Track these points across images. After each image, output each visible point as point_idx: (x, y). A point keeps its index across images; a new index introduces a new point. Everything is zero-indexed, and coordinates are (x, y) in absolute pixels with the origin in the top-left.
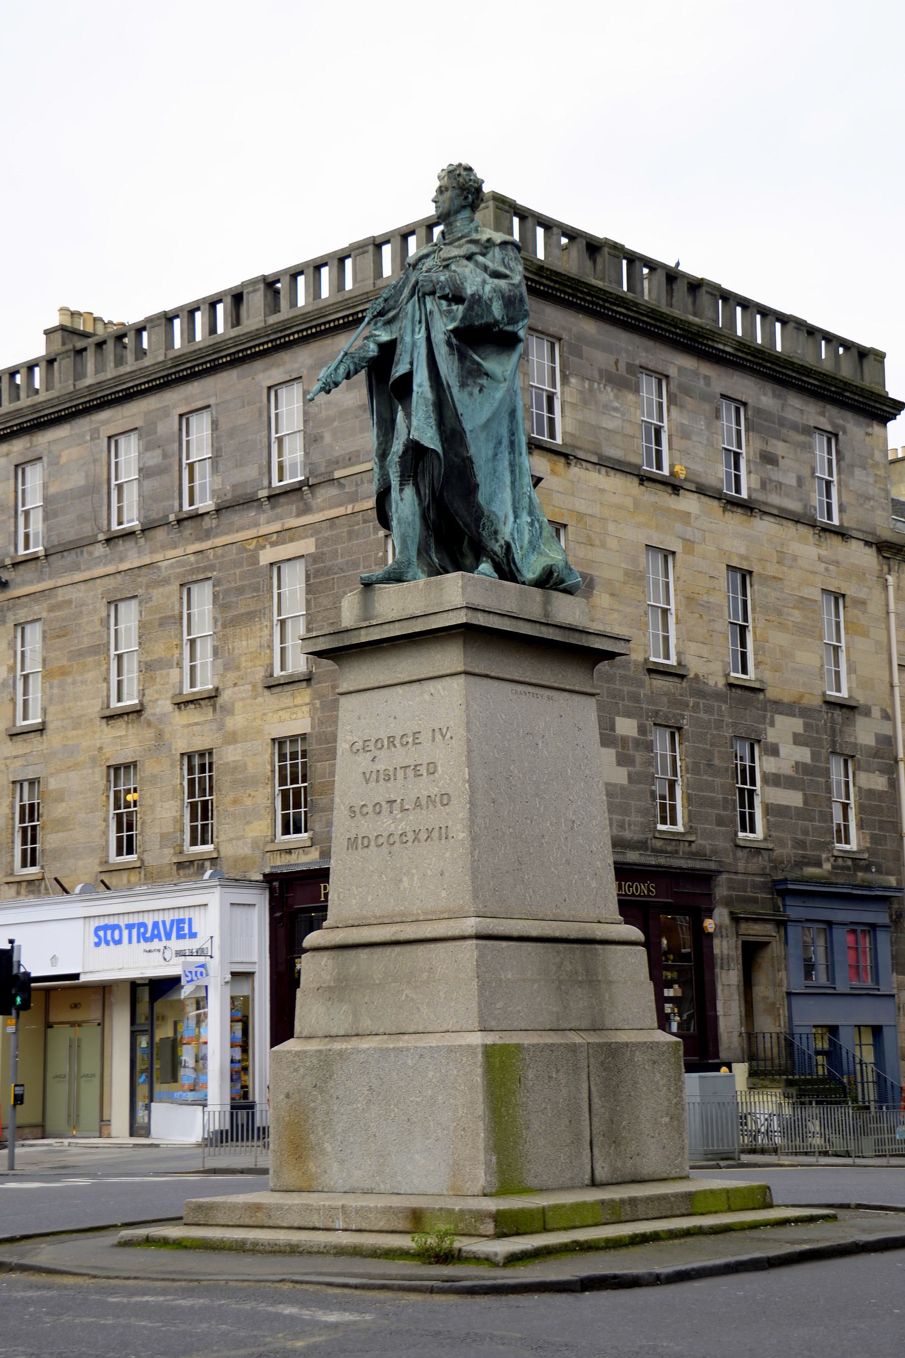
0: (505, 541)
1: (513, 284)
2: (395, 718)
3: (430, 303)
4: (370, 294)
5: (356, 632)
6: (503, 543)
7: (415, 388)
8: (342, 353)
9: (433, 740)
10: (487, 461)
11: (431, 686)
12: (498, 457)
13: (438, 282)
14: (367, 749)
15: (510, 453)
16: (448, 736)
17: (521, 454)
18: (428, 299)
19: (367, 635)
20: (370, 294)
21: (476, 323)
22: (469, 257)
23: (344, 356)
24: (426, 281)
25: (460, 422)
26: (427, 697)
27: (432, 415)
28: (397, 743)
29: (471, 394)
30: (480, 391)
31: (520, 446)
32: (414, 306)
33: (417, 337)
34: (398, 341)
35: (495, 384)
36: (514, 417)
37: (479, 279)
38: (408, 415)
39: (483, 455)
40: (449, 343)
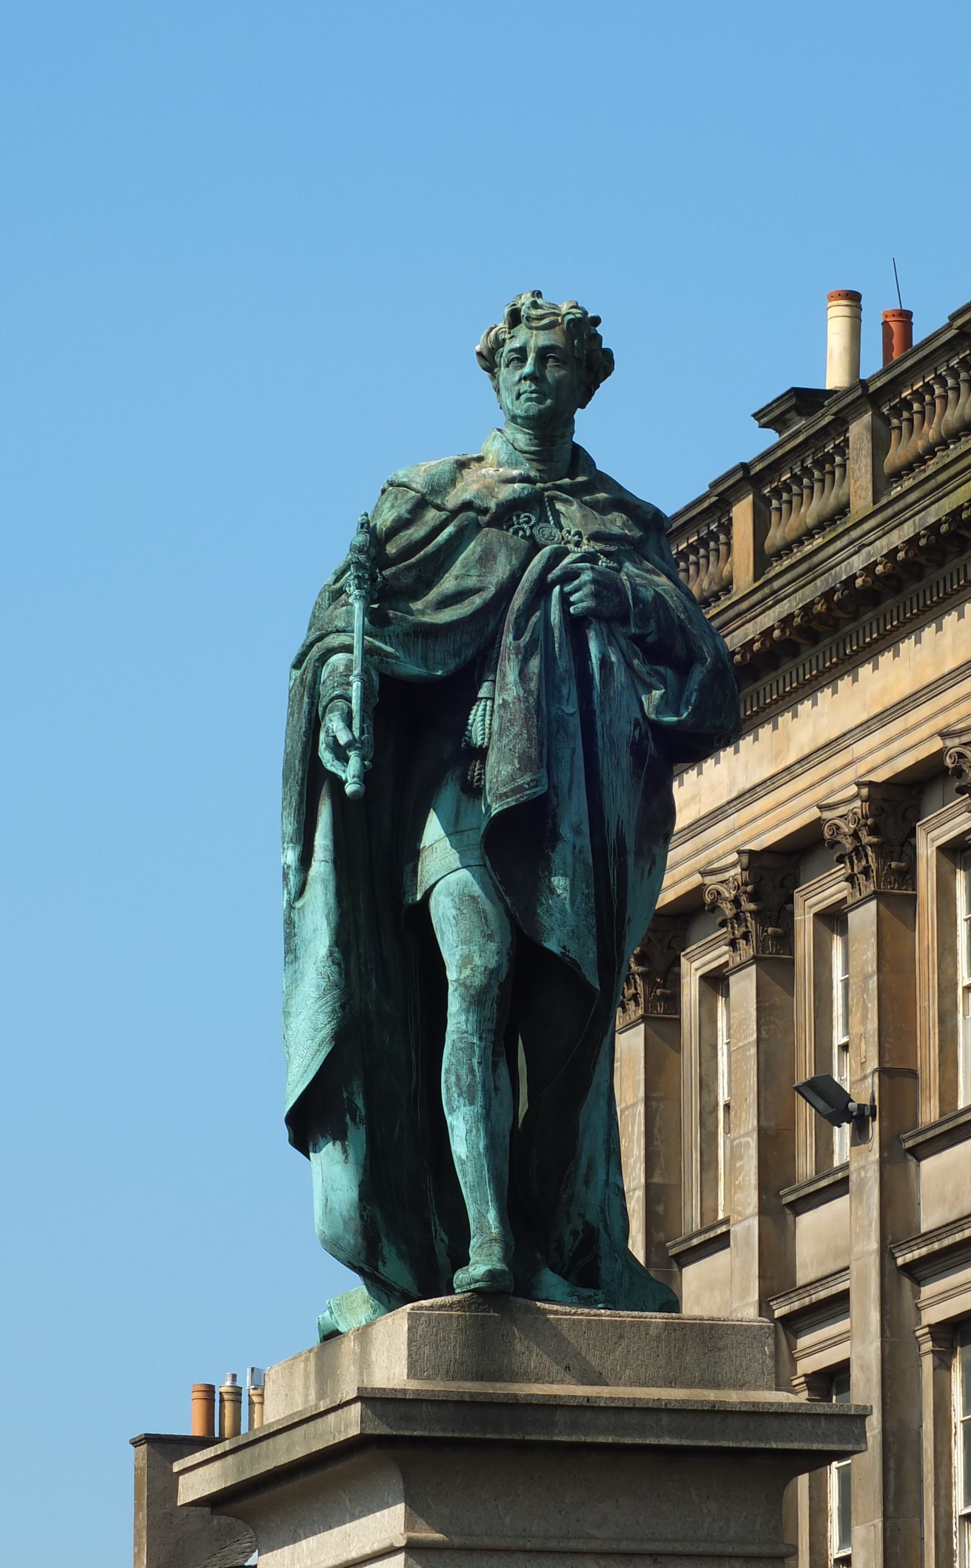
0: (586, 1224)
6: (580, 1227)
40: (637, 749)
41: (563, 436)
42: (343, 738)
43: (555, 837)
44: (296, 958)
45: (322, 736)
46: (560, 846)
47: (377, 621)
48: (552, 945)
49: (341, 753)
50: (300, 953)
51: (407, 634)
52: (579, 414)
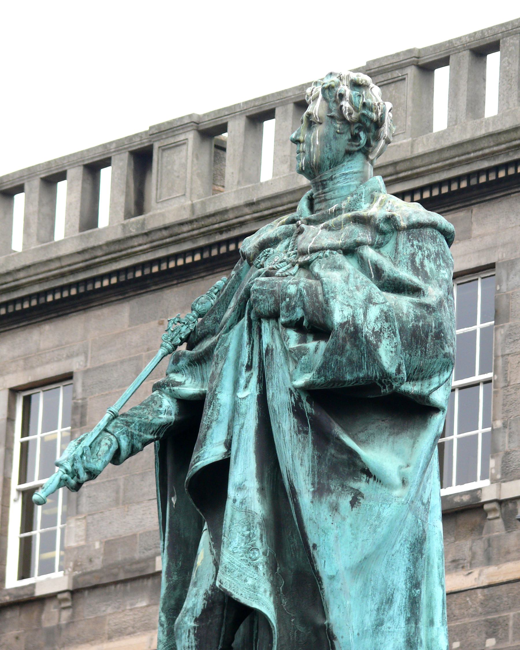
1: (427, 307)
3: (268, 335)
4: (399, 168)
7: (231, 492)
8: (107, 416)
10: (362, 635)
12: (384, 628)
13: (286, 295)
15: (408, 621)
17: (431, 623)
18: (266, 326)
20: (399, 168)
21: (348, 377)
22: (350, 251)
23: (110, 421)
24: (262, 292)
25: (311, 560)
27: (258, 544)
29: (335, 508)
30: (354, 503)
31: (430, 607)
32: (241, 336)
33: (241, 394)
34: (207, 400)
35: (382, 491)
36: (421, 552)
37: (360, 296)
38: (217, 541)
39: (355, 623)
40: (297, 411)
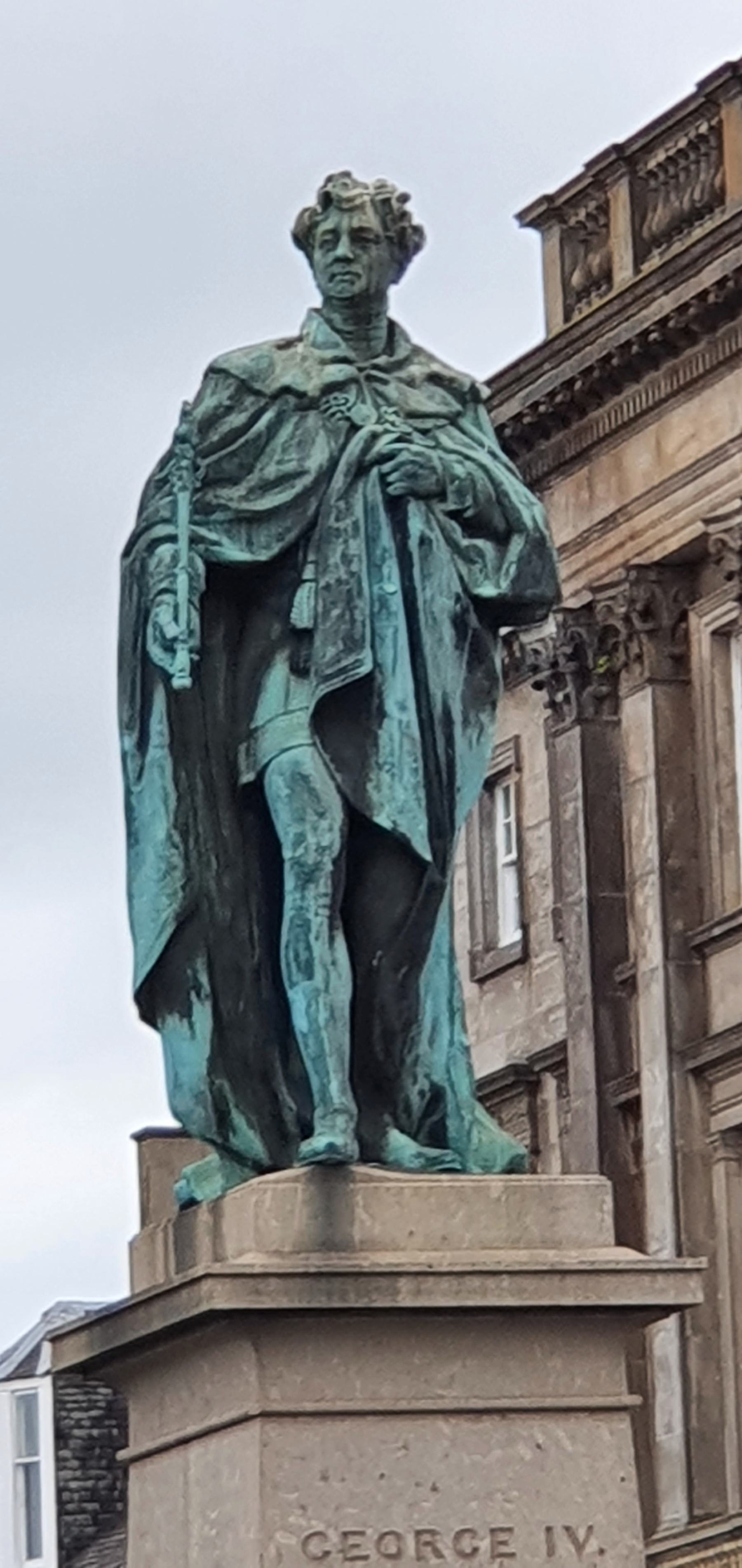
2: (434, 1489)
5: (384, 1282)
6: (427, 1087)
9: (551, 1551)
11: (538, 1429)
13: (454, 478)
14: (356, 1552)
16: (593, 1546)
19: (418, 1293)
24: (422, 466)
26: (526, 1453)
28: (445, 1544)
40: (459, 622)
41: (378, 315)
42: (171, 631)
43: (382, 714)
44: (137, 841)
45: (150, 630)
46: (386, 721)
47: (202, 511)
48: (383, 820)
49: (169, 647)
50: (141, 837)
51: (230, 521)
52: (393, 291)
